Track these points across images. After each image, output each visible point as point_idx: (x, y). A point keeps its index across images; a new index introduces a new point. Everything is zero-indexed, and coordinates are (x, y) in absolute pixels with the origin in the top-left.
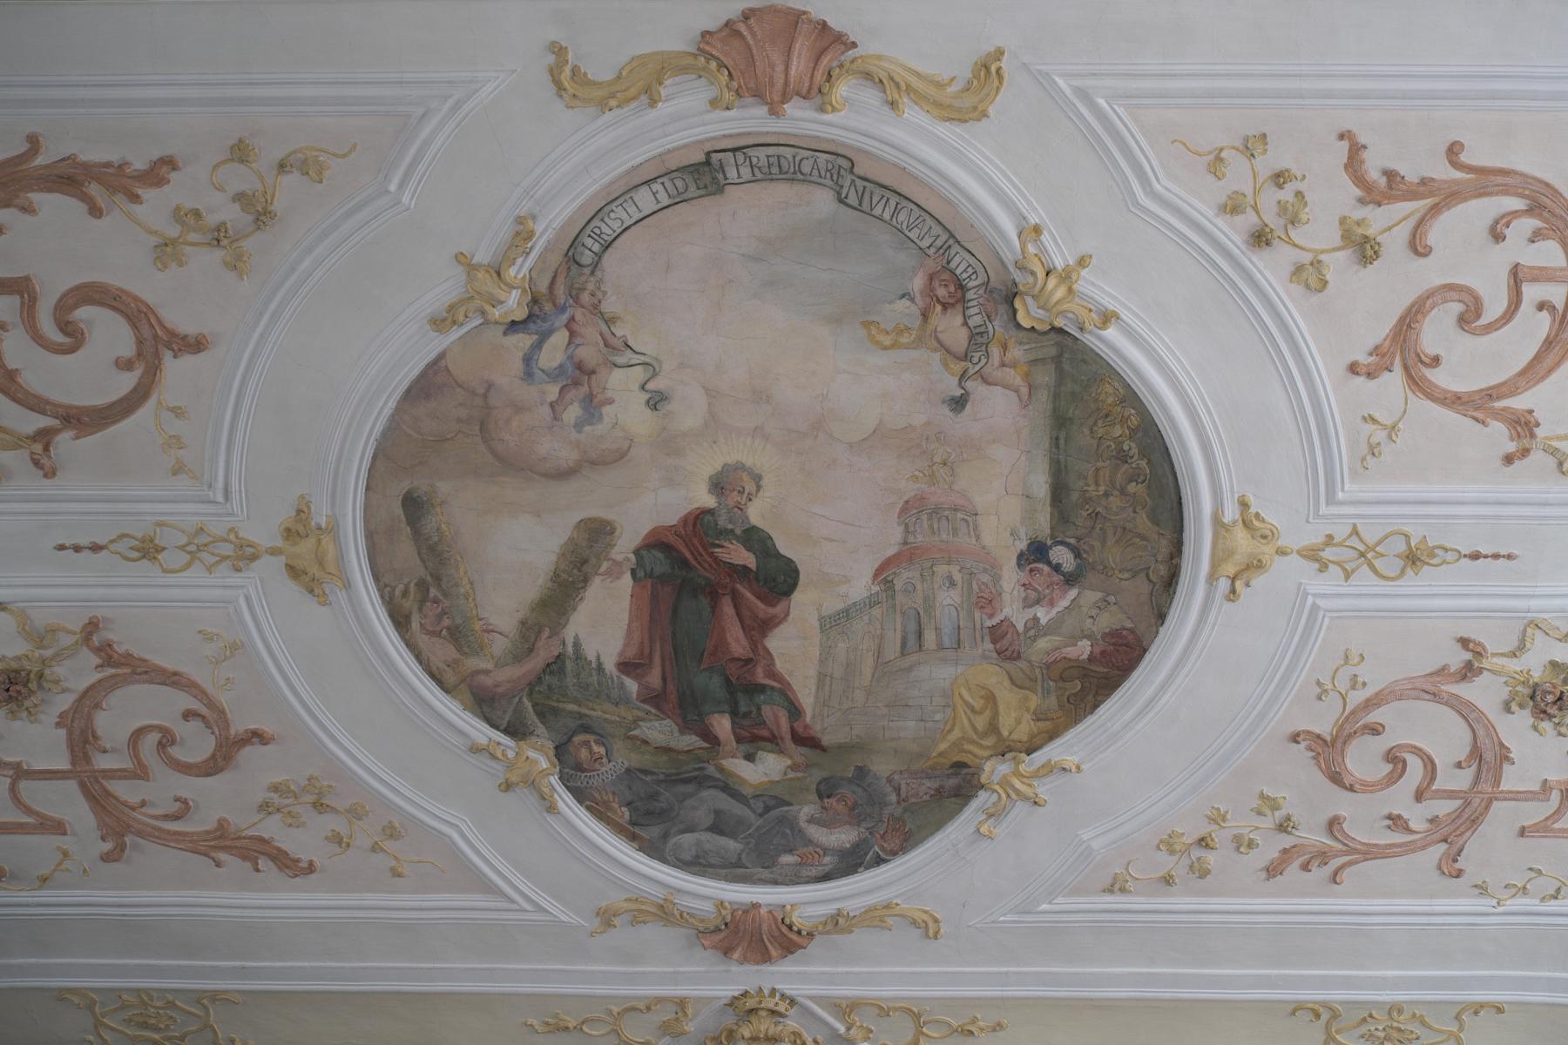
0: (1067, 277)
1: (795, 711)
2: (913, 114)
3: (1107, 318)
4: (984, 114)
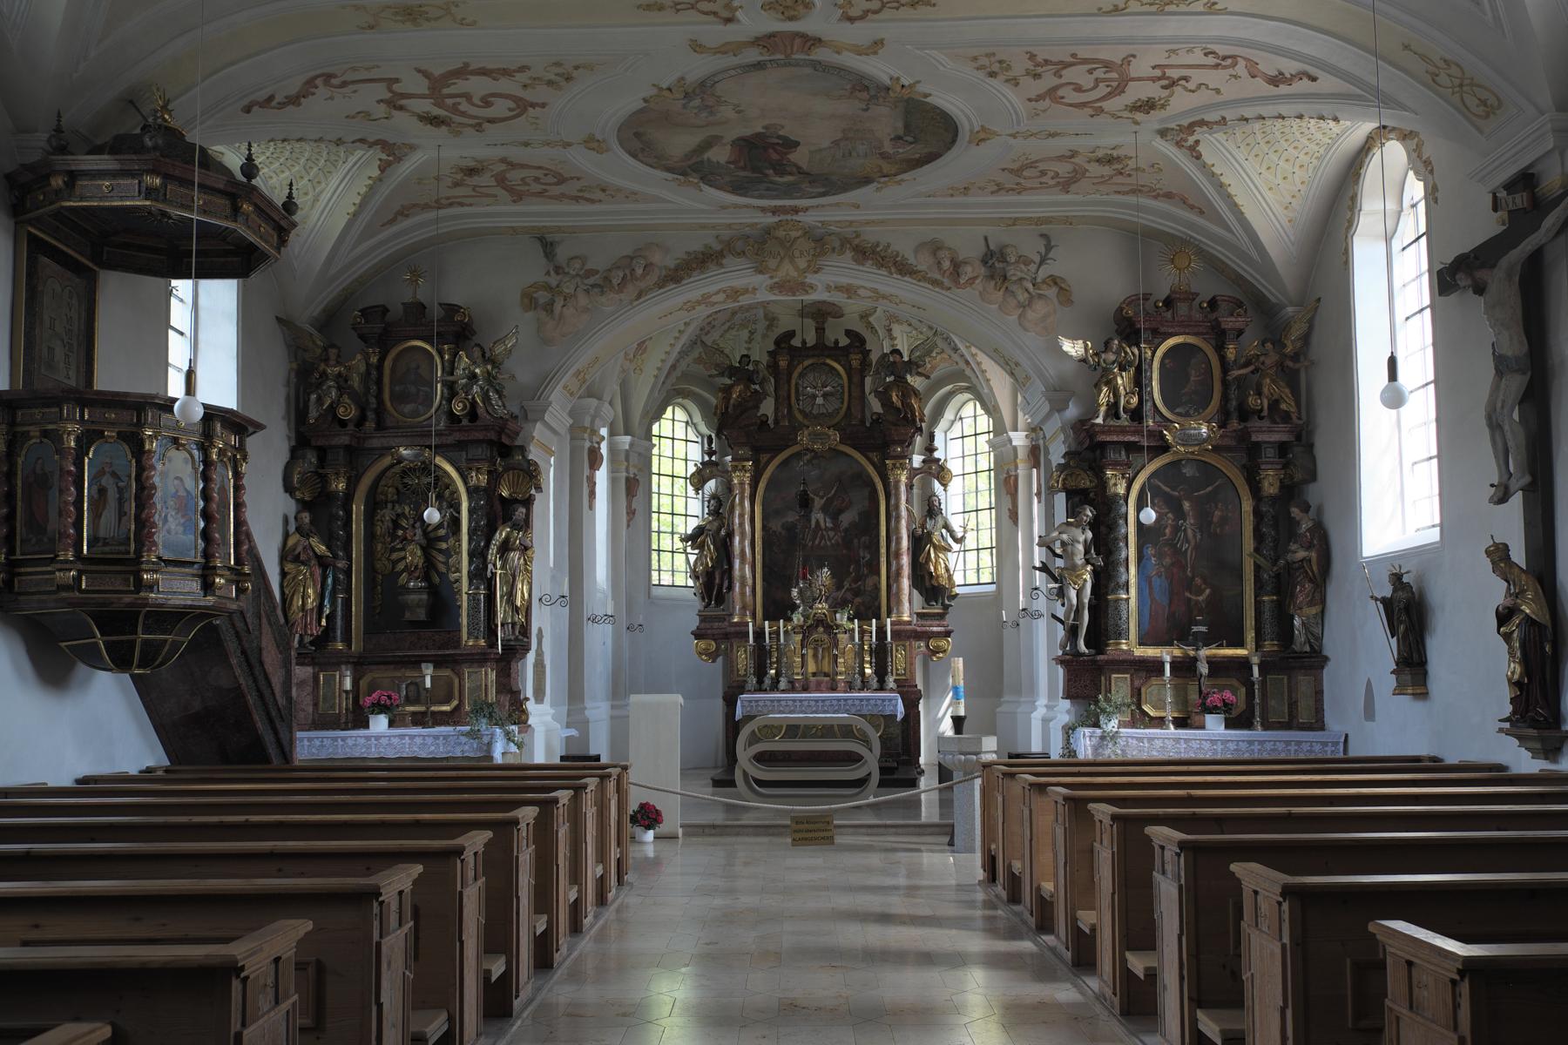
1: (799, 168)
2: (845, 53)
3: (926, 96)
4: (875, 53)
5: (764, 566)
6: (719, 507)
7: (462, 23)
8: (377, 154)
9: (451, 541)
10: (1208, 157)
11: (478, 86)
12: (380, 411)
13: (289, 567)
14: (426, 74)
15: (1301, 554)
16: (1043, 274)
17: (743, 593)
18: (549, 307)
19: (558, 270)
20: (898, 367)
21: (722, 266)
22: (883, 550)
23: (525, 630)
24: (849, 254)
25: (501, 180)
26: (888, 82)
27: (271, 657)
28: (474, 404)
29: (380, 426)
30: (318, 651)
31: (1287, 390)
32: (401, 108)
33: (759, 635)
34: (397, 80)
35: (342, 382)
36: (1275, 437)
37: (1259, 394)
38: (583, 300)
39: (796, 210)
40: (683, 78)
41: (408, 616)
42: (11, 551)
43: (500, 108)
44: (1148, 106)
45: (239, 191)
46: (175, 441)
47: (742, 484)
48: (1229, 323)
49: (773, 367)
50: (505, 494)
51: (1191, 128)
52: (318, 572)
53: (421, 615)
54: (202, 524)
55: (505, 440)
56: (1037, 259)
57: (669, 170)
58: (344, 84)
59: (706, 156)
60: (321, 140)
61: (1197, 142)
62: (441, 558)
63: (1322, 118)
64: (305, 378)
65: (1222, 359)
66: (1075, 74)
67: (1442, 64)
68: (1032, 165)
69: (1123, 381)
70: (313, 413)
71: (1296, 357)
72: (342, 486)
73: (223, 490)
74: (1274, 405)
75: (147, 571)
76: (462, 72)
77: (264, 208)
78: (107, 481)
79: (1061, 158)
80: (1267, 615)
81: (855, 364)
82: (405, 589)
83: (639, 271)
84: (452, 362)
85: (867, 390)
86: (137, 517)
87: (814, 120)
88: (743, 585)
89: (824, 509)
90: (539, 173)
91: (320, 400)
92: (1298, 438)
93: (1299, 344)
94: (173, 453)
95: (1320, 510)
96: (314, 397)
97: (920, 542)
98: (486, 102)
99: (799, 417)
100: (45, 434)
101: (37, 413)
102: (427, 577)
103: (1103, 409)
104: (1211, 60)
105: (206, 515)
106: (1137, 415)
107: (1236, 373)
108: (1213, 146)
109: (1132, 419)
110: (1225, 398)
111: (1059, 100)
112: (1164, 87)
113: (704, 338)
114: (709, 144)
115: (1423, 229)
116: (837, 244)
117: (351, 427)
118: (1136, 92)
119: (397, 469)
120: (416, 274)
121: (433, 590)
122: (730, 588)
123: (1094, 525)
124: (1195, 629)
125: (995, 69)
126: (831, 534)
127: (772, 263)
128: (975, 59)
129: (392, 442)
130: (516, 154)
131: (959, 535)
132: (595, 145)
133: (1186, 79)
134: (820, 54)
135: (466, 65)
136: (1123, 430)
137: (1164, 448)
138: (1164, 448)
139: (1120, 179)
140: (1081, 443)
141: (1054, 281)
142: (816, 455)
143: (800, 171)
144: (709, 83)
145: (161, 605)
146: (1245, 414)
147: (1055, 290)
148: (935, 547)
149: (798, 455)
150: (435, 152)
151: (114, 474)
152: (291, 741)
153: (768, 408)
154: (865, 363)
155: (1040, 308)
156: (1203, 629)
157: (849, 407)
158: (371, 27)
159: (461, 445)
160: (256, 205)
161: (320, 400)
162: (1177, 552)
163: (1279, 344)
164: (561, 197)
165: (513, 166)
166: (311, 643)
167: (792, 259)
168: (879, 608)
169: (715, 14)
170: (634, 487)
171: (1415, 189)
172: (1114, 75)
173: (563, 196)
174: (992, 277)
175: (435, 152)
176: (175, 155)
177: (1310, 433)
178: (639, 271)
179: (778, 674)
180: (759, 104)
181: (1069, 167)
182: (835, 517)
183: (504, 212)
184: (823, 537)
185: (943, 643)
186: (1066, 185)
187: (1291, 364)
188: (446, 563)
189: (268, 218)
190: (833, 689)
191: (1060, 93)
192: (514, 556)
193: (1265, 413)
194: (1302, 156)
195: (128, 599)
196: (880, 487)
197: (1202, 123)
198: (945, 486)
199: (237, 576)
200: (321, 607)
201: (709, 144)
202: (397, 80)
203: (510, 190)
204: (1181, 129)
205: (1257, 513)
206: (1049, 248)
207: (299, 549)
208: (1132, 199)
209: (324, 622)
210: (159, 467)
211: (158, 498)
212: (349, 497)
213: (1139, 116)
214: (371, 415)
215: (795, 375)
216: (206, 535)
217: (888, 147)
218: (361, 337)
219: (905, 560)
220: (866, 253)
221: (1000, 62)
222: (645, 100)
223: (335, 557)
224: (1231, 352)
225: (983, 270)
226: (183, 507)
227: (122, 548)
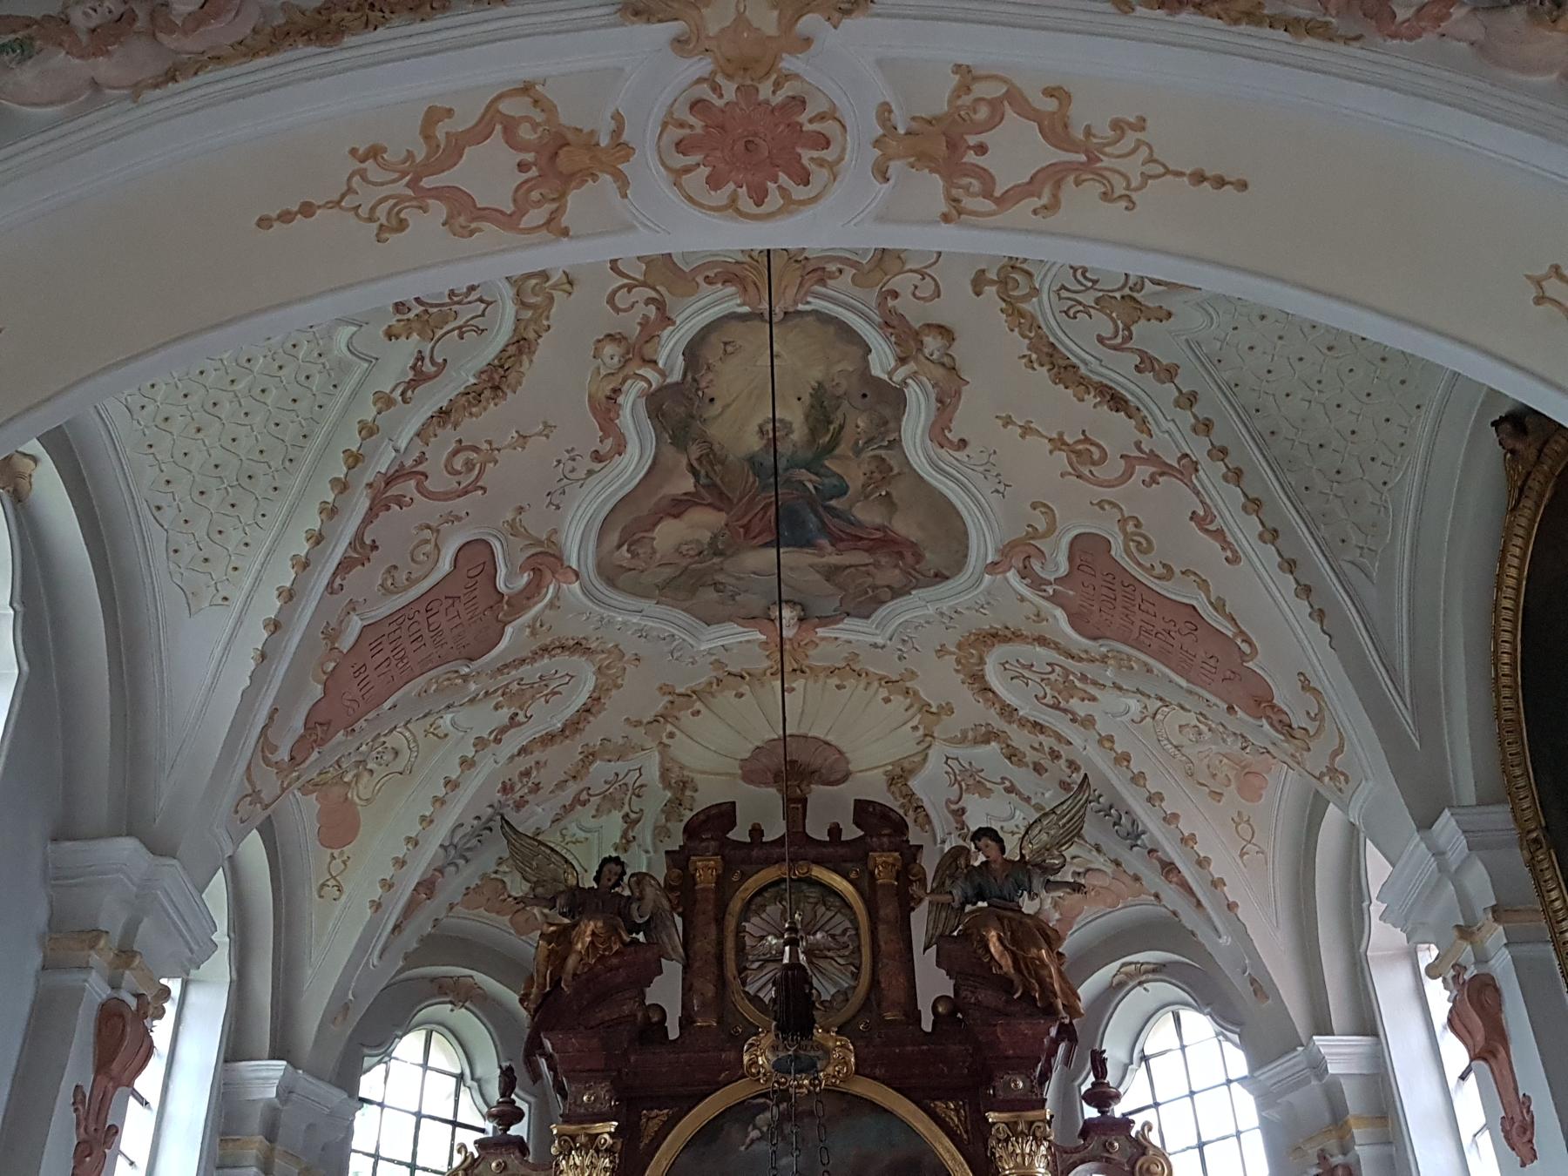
20: (995, 883)
49: (681, 886)
81: (884, 877)
113: (512, 816)
142: (794, 1113)
149: (743, 1112)
153: (666, 991)
157: (875, 982)
215: (736, 905)
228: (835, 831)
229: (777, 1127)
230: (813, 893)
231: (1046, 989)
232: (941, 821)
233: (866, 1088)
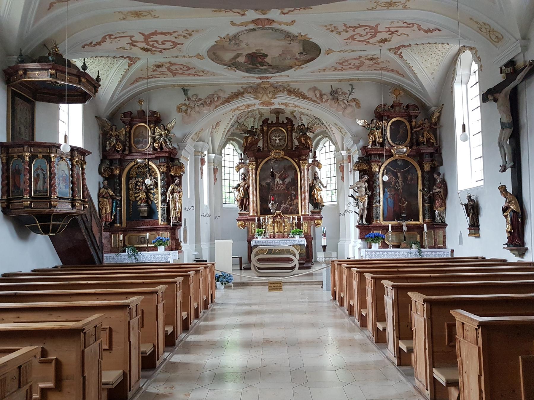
0: (305, 35)
5: (260, 197)
6: (245, 178)
7: (154, 17)
8: (127, 61)
9: (155, 190)
10: (405, 58)
11: (160, 38)
12: (130, 147)
13: (101, 199)
14: (143, 34)
15: (438, 190)
16: (351, 97)
17: (253, 206)
18: (186, 112)
19: (189, 99)
21: (243, 97)
22: (299, 191)
23: (180, 219)
24: (286, 92)
25: (169, 69)
26: (297, 35)
27: (95, 229)
28: (161, 144)
29: (130, 152)
30: (111, 227)
31: (432, 136)
32: (135, 46)
33: (259, 220)
34: (133, 36)
35: (118, 139)
36: (428, 151)
37: (423, 136)
38: (197, 109)
39: (268, 78)
40: (228, 34)
41: (141, 215)
42: (9, 195)
43: (168, 45)
44: (384, 41)
45: (81, 75)
46: (62, 158)
47: (252, 170)
48: (413, 113)
49: (262, 130)
50: (172, 174)
51: (399, 48)
52: (111, 200)
53: (146, 215)
54: (71, 185)
55: (172, 156)
56: (349, 93)
57: (225, 65)
58: (116, 38)
59: (237, 60)
60: (108, 56)
61: (401, 52)
62: (152, 196)
63: (443, 44)
64: (105, 136)
65: (411, 125)
66: (360, 31)
67: (483, 24)
68: (347, 61)
69: (377, 133)
70: (108, 148)
71: (435, 124)
72: (118, 172)
73: (78, 174)
74: (428, 140)
75: (53, 201)
76: (155, 33)
77: (89, 79)
78: (39, 172)
79: (356, 59)
80: (426, 211)
82: (140, 206)
83: (216, 99)
84: (154, 130)
85: (293, 138)
86: (50, 183)
87: (273, 48)
88: (253, 203)
89: (279, 178)
90: (182, 67)
91: (110, 143)
92: (437, 151)
93: (436, 120)
94: (61, 162)
95: (444, 175)
96: (108, 142)
97: (312, 188)
98: (163, 43)
99: (271, 147)
100: (19, 156)
101: (16, 150)
102: (147, 202)
103: (371, 143)
104: (405, 25)
105: (72, 182)
106: (382, 144)
107: (415, 130)
108: (405, 53)
109: (381, 146)
110: (412, 138)
111: (354, 39)
112: (390, 34)
114: (238, 56)
115: (477, 81)
116: (282, 89)
117: (120, 152)
118: (380, 36)
119: (136, 166)
120: (141, 101)
121: (149, 206)
122: (249, 204)
123: (368, 182)
124: (402, 215)
125: (333, 29)
126: (282, 186)
127: (260, 96)
128: (326, 26)
129: (135, 157)
130: (174, 60)
131: (325, 186)
132: (200, 57)
133: (397, 31)
134: (275, 26)
135: (156, 31)
136: (378, 150)
137: (391, 155)
138: (391, 155)
139: (376, 65)
140: (364, 154)
141: (354, 100)
142: (277, 160)
143: (268, 65)
144: (237, 36)
145: (58, 212)
146: (418, 144)
147: (355, 103)
148: (317, 190)
150: (146, 60)
151: (42, 169)
152: (103, 257)
154: (292, 129)
155: (349, 110)
156: (405, 215)
158: (124, 19)
159: (157, 158)
160: (87, 79)
161: (110, 143)
162: (396, 190)
163: (430, 120)
164: (189, 74)
165: (172, 64)
166: (109, 224)
167: (267, 94)
168: (298, 210)
169: (239, 13)
170: (216, 171)
171: (475, 67)
172: (373, 31)
173: (190, 74)
174: (334, 99)
175: (146, 60)
176: (59, 63)
177: (440, 150)
178: (216, 99)
179: (265, 232)
180: (255, 43)
181: (359, 62)
182: (283, 180)
183: (170, 80)
184: (279, 187)
185: (320, 221)
186: (358, 68)
187: (433, 126)
188: (153, 197)
189: (91, 84)
190: (283, 237)
191: (355, 37)
192: (176, 195)
193: (425, 143)
194: (437, 56)
195: (47, 210)
196: (298, 170)
197: (403, 46)
198: (320, 169)
199: (83, 202)
200: (112, 212)
201: (238, 56)
202: (133, 36)
203: (172, 72)
204: (396, 48)
205: (423, 176)
206: (352, 89)
207: (104, 193)
208: (380, 72)
209: (113, 217)
210: (56, 167)
211: (56, 176)
212: (120, 175)
213: (381, 44)
214: (127, 148)
215: (269, 133)
216: (72, 189)
217: (298, 56)
218: (123, 122)
219: (307, 194)
220: (291, 92)
221: (335, 27)
222: (216, 42)
223: (116, 196)
224: (414, 123)
225: (330, 97)
226: (65, 180)
227: (45, 194)
228: (283, 122)
229: (274, 162)
230: (280, 131)
231: (309, 145)
232: (298, 118)
233: (286, 157)
